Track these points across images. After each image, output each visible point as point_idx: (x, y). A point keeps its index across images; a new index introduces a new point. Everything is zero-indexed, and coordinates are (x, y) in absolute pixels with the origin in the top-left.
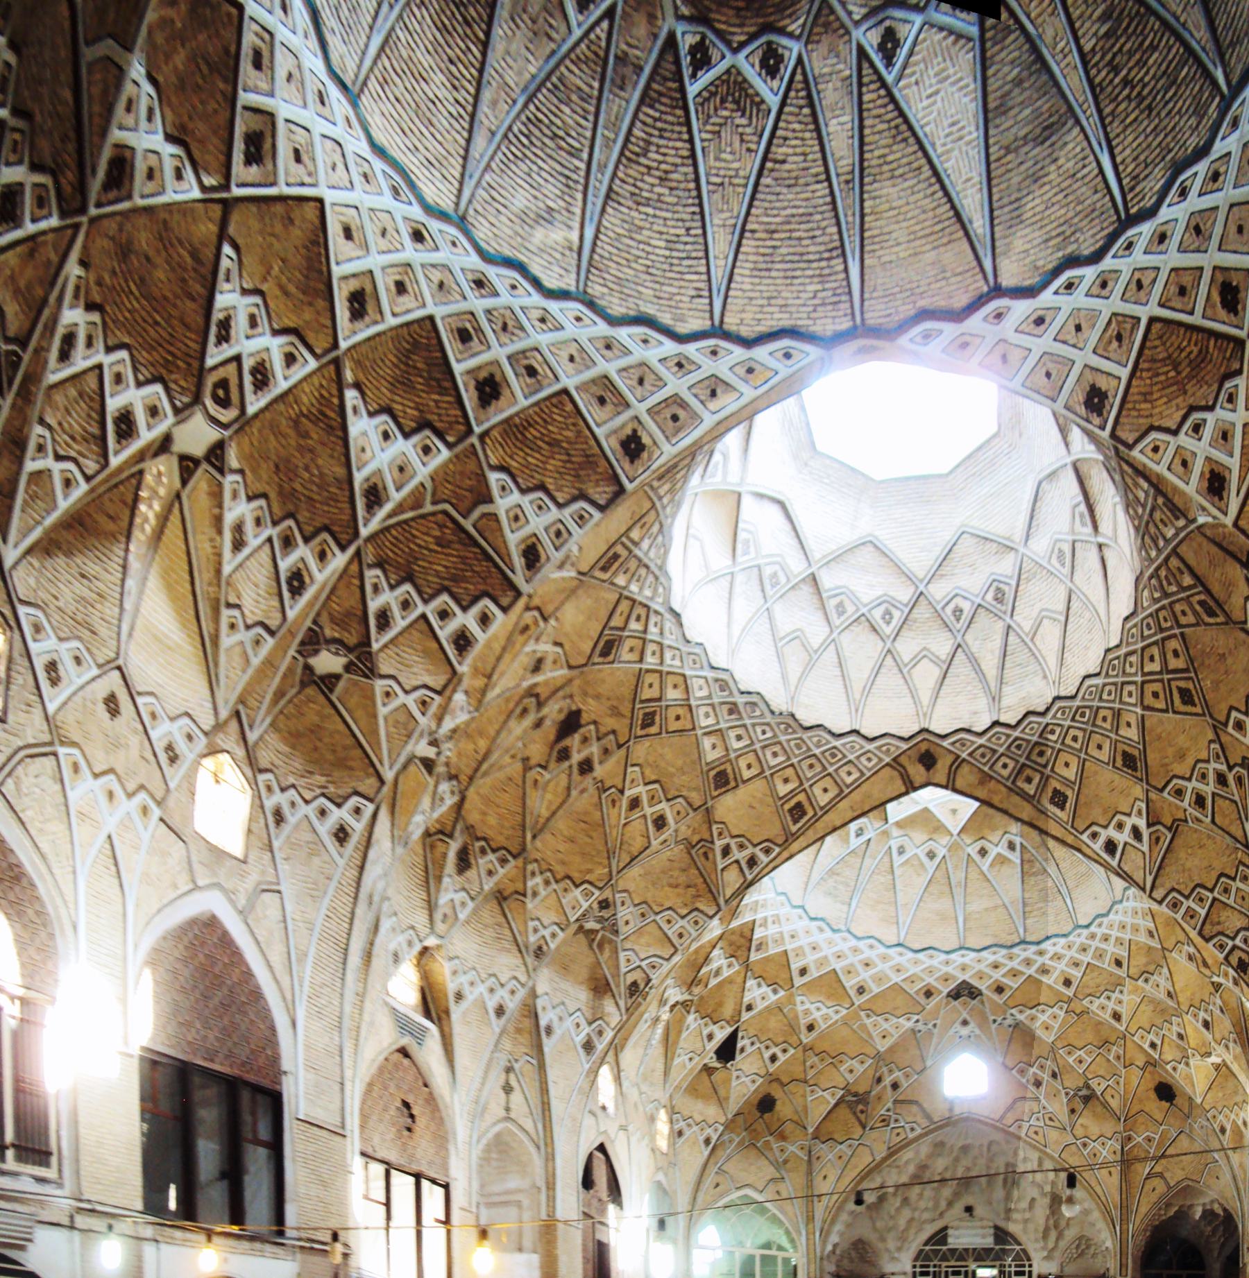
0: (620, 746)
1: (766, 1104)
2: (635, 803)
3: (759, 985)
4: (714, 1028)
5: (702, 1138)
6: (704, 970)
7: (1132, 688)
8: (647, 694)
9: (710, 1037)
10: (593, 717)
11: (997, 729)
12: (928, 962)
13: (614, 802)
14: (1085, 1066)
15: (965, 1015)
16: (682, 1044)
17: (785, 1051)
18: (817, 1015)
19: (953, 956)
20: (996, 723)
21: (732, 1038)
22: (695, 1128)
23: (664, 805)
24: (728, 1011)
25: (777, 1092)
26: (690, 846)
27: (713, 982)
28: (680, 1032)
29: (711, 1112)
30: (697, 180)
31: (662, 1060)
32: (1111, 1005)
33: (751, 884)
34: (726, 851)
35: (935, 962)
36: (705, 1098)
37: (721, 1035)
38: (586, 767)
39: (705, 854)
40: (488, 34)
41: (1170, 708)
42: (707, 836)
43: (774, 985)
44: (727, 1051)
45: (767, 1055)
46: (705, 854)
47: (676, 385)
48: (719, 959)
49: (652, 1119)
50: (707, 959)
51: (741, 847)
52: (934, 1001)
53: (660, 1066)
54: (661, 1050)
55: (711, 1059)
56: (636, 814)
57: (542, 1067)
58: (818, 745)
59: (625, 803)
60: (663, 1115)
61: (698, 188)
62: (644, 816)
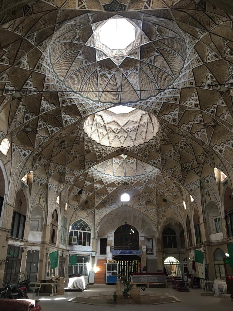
0: (71, 146)
1: (86, 202)
2: (72, 154)
3: (88, 182)
4: (79, 188)
5: (74, 208)
6: (79, 179)
7: (158, 142)
8: (77, 139)
9: (78, 190)
10: (67, 141)
11: (135, 147)
12: (119, 179)
13: (68, 154)
14: (148, 196)
15: (125, 187)
16: (72, 191)
17: (91, 193)
18: (98, 187)
19: (123, 178)
20: (134, 146)
21: (81, 191)
22: (72, 206)
23: (77, 155)
24: (81, 186)
25: (89, 200)
26: (80, 161)
27: (80, 181)
28: (72, 189)
29: (76, 203)
30: (98, 84)
31: (68, 194)
32: (153, 186)
33: (91, 167)
34: (87, 162)
35: (120, 179)
36: (75, 201)
37: (79, 190)
38: (64, 148)
39: (83, 162)
40: (72, 64)
41: (165, 144)
42: (84, 160)
43: (90, 182)
44: (80, 193)
45: (88, 194)
46: (83, 162)
47: (92, 106)
48: (81, 177)
49: (65, 204)
50: (79, 177)
51: (89, 162)
52: (119, 185)
53: (68, 195)
54: (68, 192)
55: (77, 194)
56: (72, 155)
57: (47, 195)
58: (104, 148)
59: (70, 154)
60: (67, 204)
61: (98, 85)
62: (73, 156)
